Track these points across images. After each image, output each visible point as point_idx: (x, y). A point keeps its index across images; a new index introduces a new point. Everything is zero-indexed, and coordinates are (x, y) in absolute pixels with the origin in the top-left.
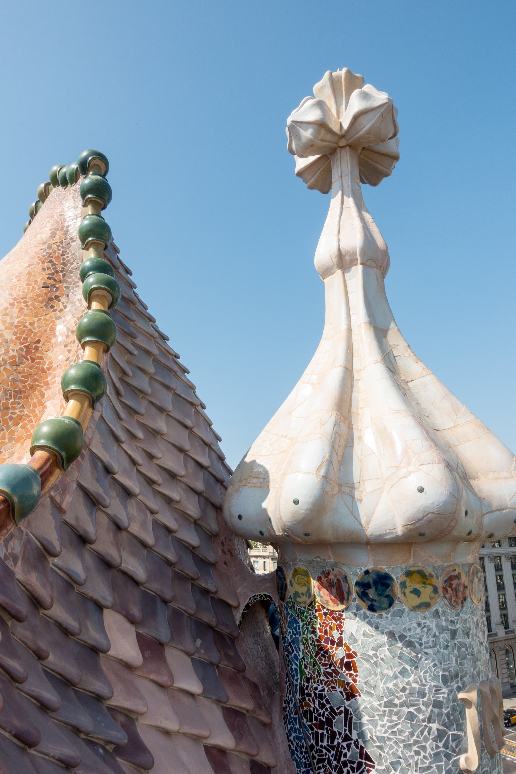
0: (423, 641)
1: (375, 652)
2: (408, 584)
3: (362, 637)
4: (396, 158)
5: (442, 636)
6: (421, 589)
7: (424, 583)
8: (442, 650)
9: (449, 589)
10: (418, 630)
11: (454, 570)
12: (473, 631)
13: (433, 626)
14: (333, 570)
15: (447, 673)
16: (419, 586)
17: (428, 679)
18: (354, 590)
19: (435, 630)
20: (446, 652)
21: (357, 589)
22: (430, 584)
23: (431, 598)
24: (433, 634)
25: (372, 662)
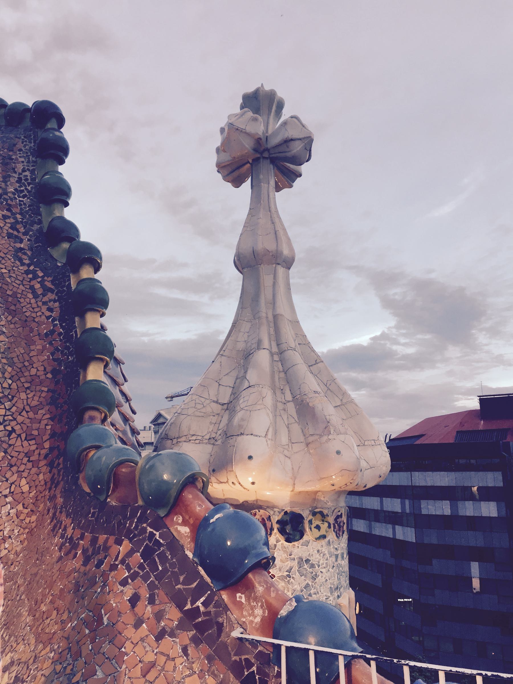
0: (320, 564)
1: (288, 573)
2: (313, 522)
3: (280, 563)
4: (300, 175)
5: (331, 559)
6: (321, 525)
7: (323, 521)
8: (331, 570)
9: (336, 525)
10: (318, 556)
11: (339, 511)
12: (345, 556)
13: (326, 552)
14: (259, 511)
15: (332, 586)
16: (319, 523)
17: (322, 590)
18: (276, 526)
19: (328, 555)
20: (333, 571)
21: (278, 526)
22: (326, 522)
23: (327, 532)
24: (326, 558)
25: (286, 580)
